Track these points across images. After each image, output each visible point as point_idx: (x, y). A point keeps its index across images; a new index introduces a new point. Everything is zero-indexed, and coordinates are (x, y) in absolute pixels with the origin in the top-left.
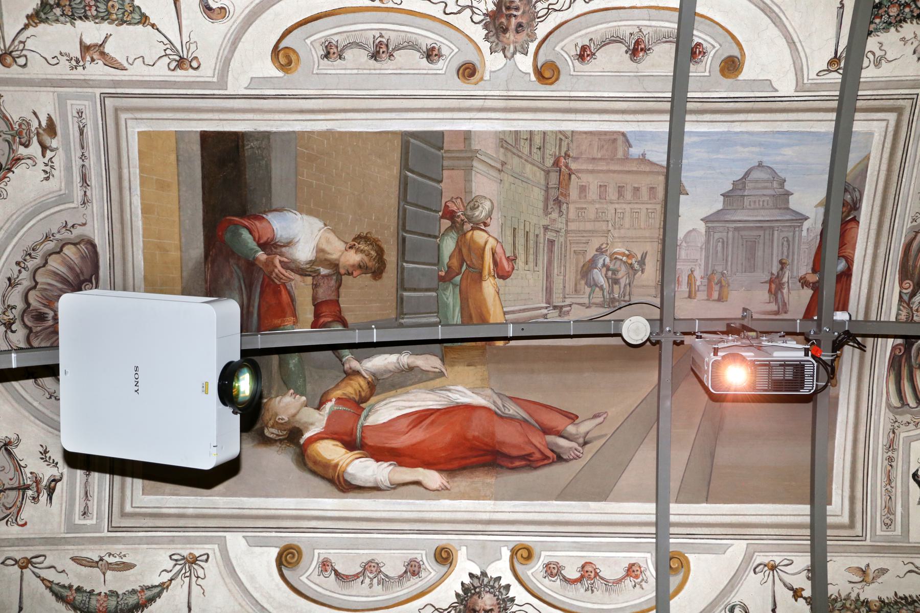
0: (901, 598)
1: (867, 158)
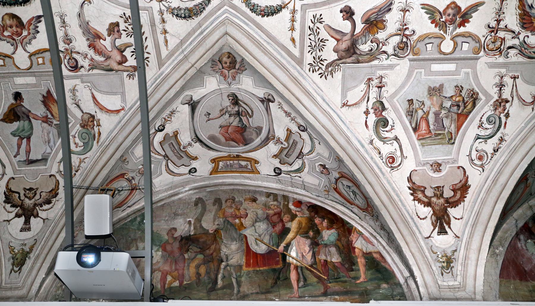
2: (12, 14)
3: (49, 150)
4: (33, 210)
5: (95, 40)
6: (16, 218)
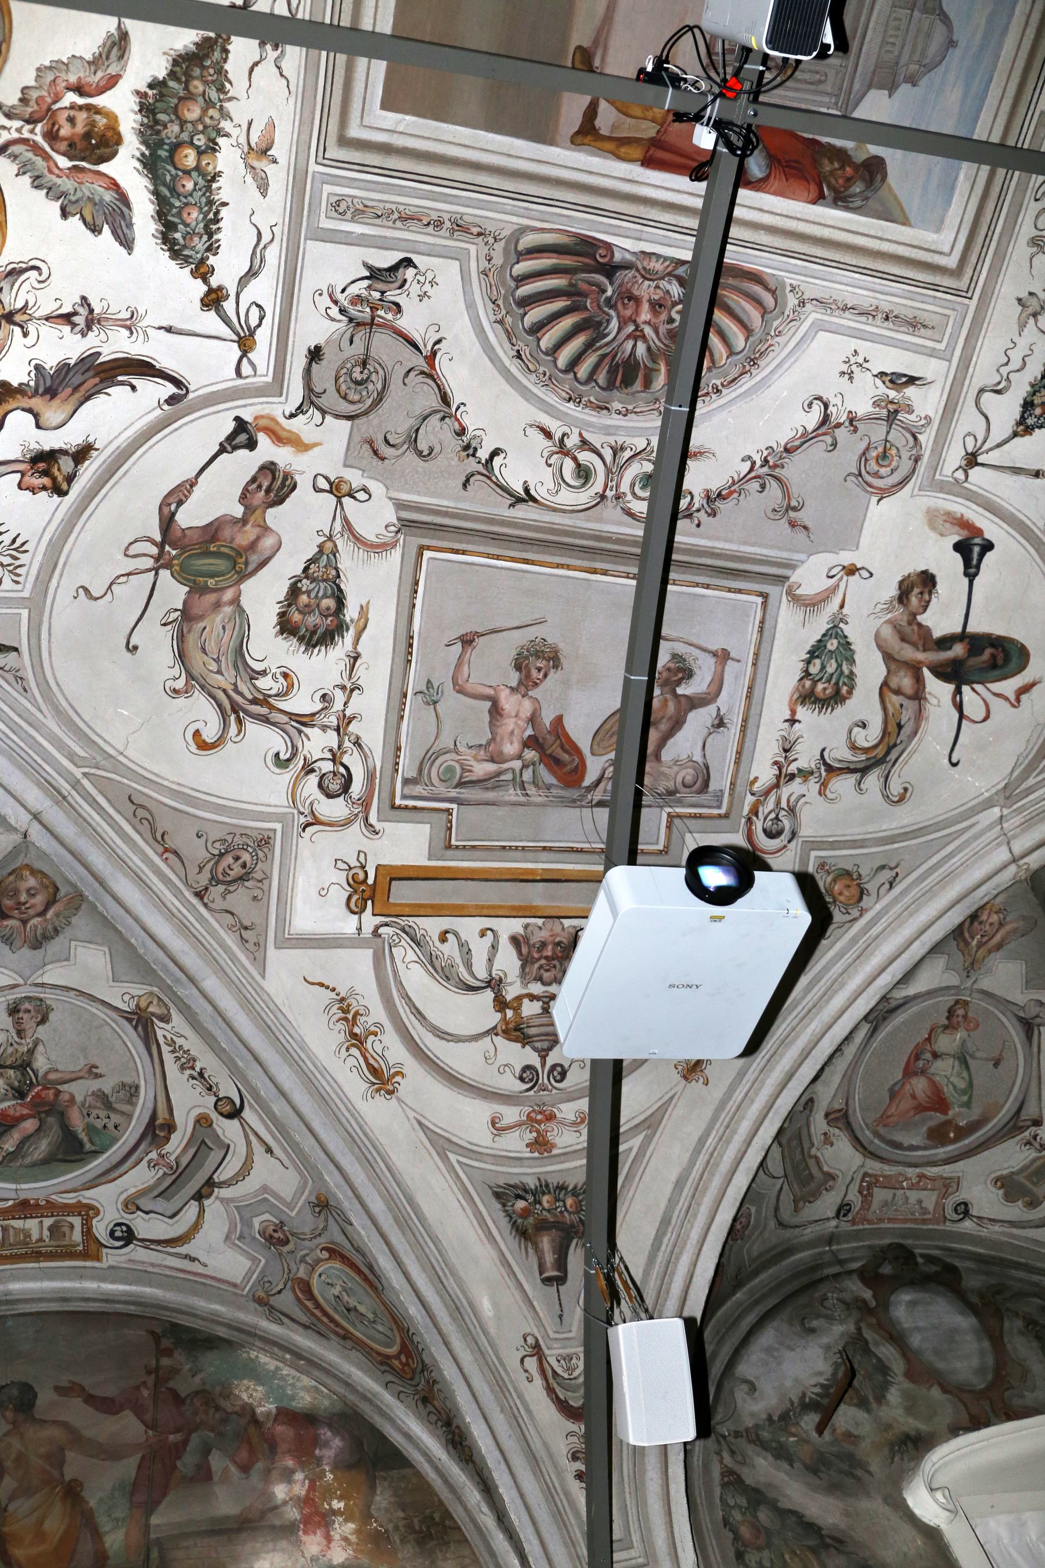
0: (217, 213)
1: (905, 222)
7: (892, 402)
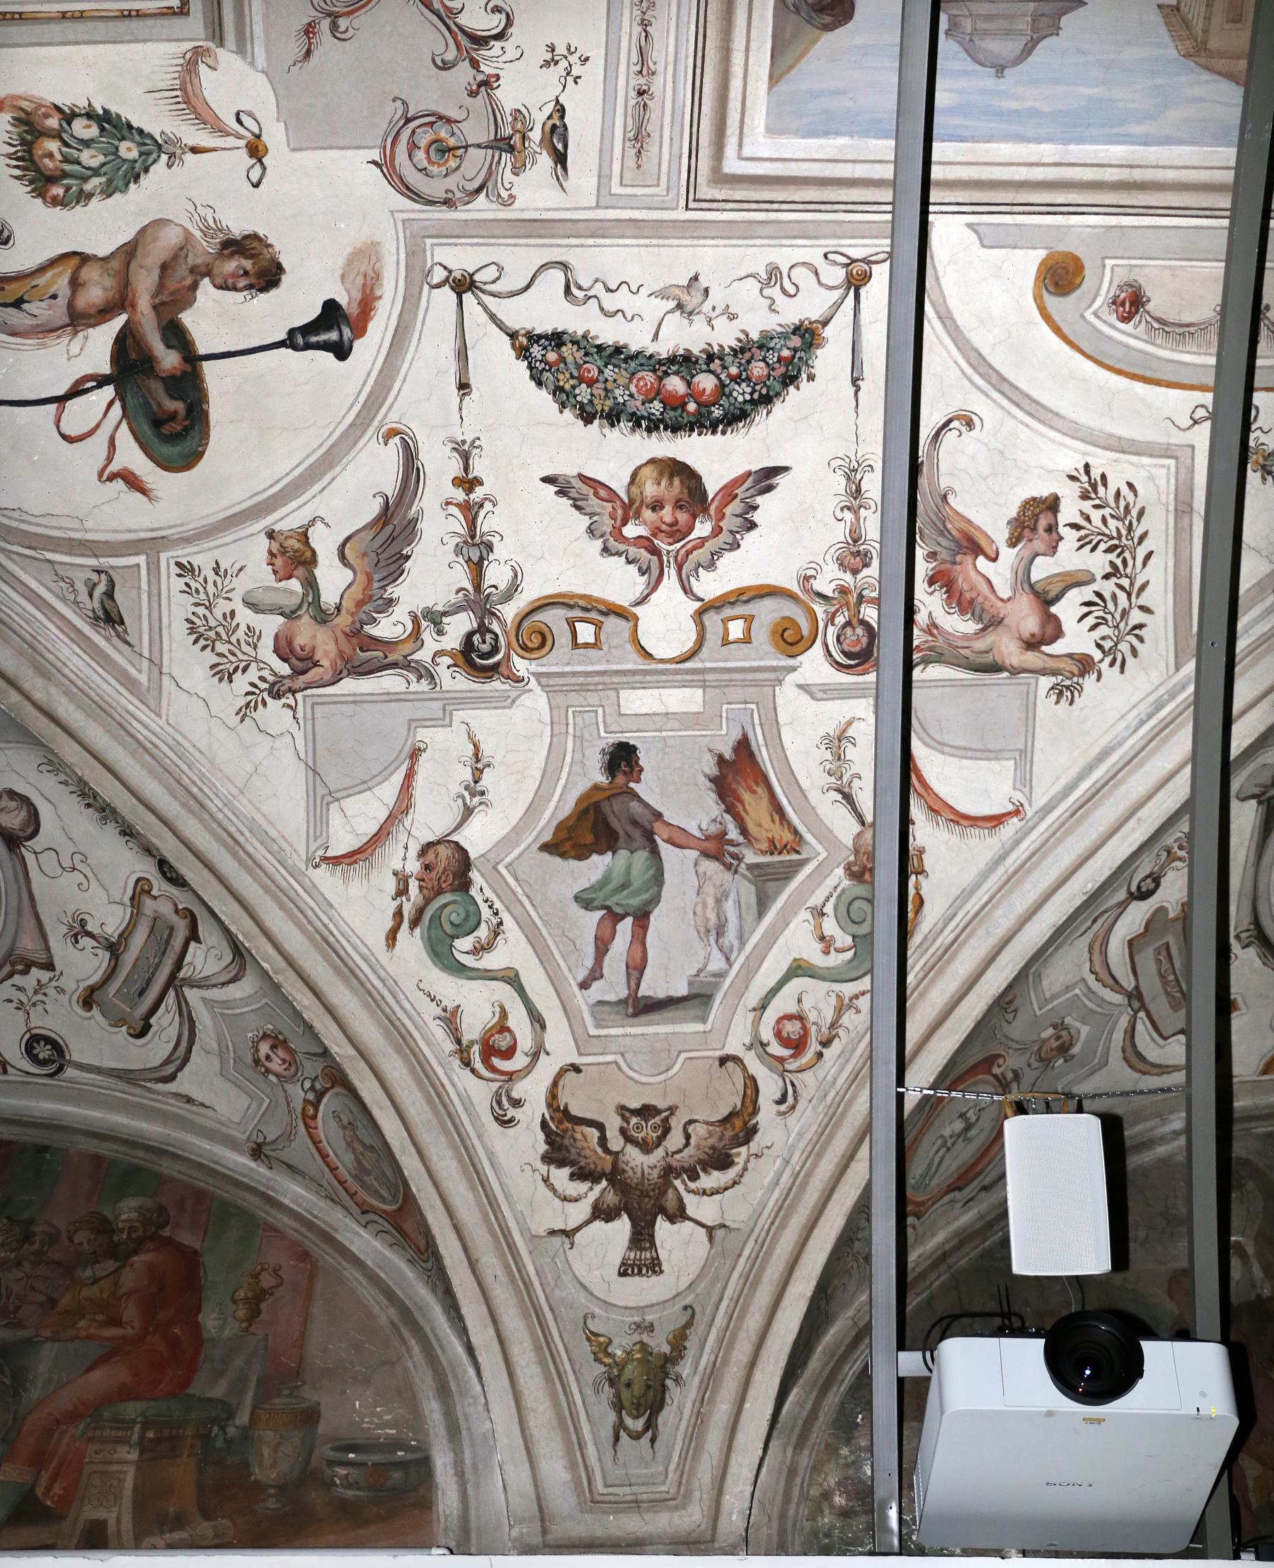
1: (774, 79)
2: (673, 461)
3: (717, 963)
4: (663, 1193)
5: (958, 558)
6: (598, 1224)
7: (524, 138)
